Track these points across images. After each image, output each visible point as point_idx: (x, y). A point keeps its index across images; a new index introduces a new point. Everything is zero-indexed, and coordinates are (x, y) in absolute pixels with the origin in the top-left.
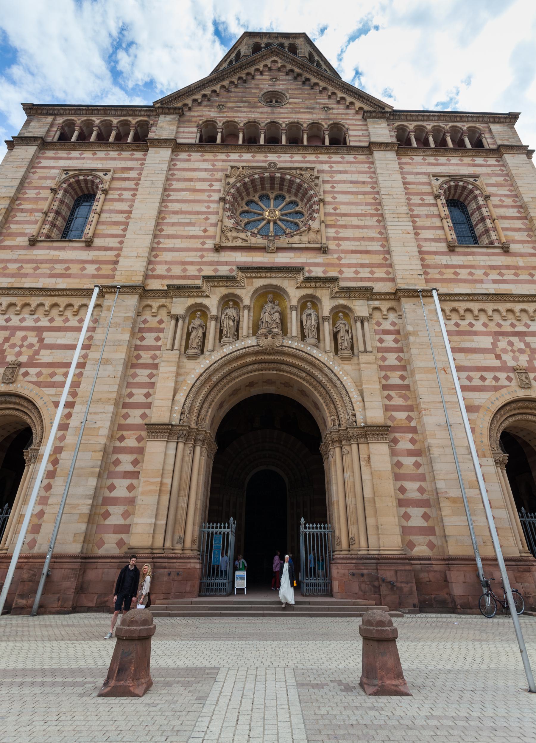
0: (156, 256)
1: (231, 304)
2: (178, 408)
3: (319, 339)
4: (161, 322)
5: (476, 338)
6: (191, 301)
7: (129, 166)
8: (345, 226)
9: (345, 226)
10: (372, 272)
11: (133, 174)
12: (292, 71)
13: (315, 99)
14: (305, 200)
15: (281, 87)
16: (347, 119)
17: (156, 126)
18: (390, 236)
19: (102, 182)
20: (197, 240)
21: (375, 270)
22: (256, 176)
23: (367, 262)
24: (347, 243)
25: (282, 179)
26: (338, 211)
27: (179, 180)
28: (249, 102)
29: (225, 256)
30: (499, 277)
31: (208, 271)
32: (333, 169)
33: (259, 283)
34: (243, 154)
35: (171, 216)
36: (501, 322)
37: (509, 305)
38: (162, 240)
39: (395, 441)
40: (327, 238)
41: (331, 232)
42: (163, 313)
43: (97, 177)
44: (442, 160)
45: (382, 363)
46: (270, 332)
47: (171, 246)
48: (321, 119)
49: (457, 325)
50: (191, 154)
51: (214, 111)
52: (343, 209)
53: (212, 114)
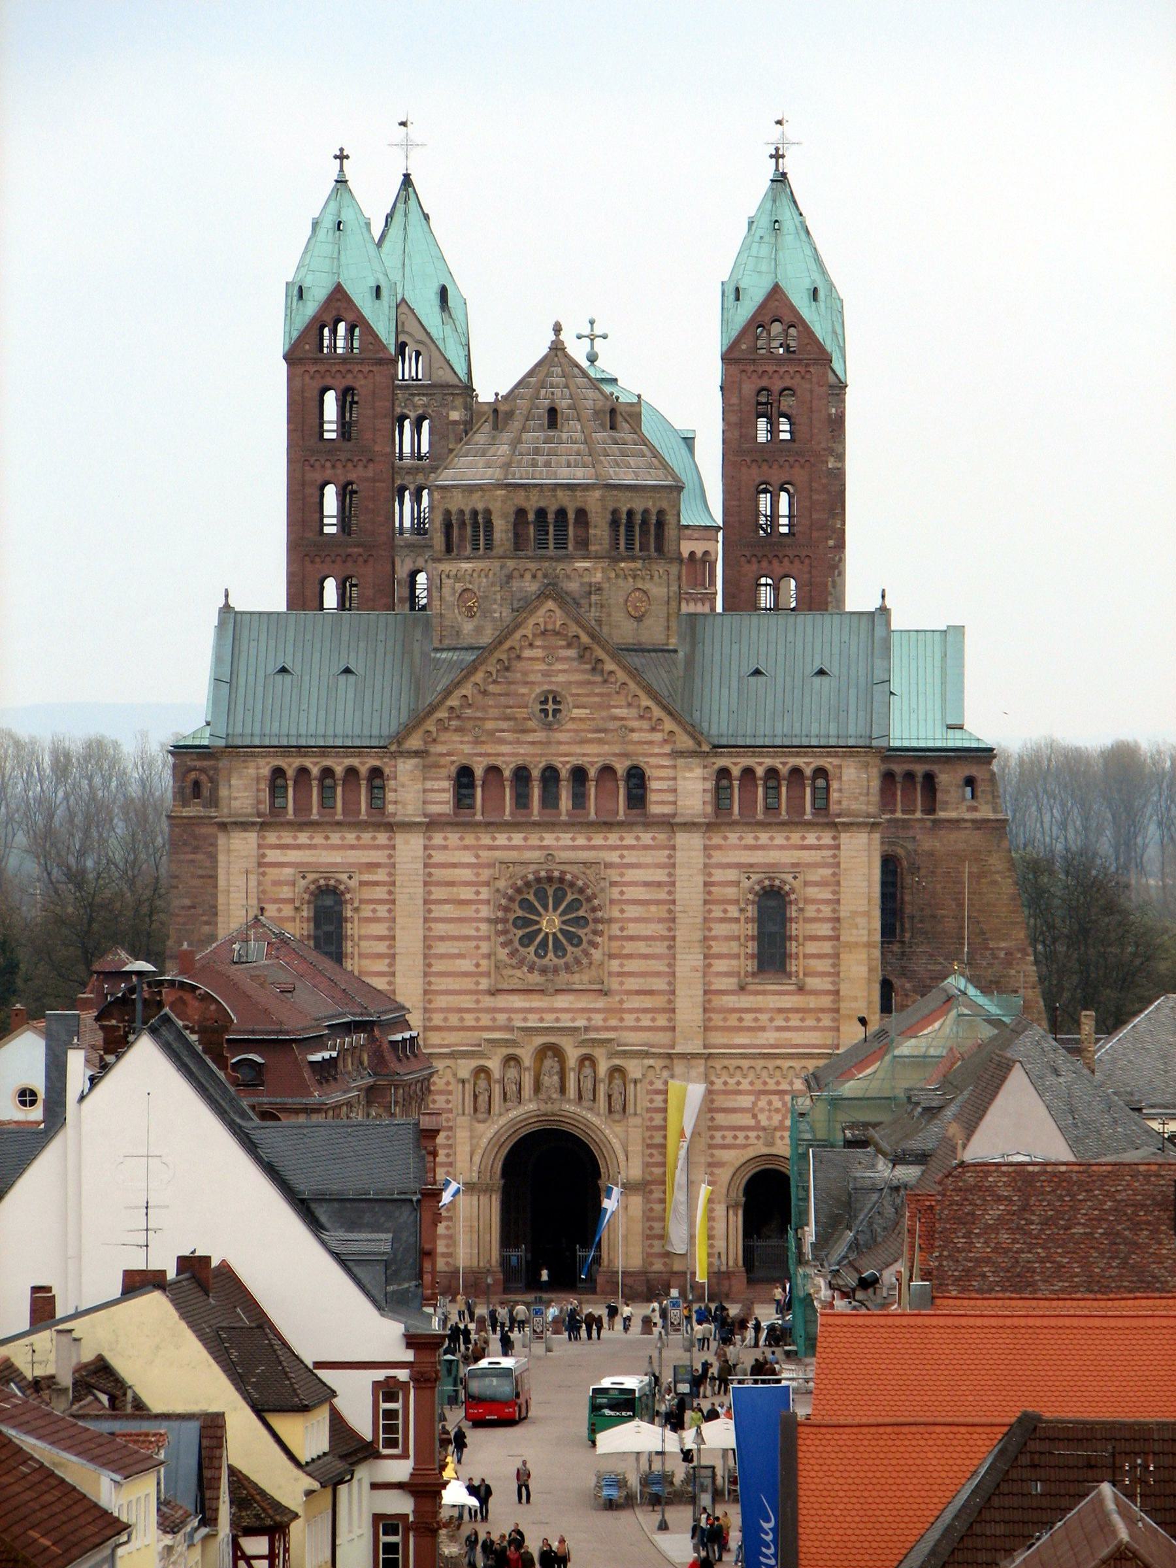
0: (430, 1002)
1: (512, 1063)
2: (475, 1168)
3: (594, 1100)
4: (448, 1083)
5: (739, 1098)
6: (474, 1063)
7: (375, 861)
8: (630, 956)
9: (630, 956)
10: (654, 1020)
11: (381, 875)
12: (577, 637)
13: (610, 707)
14: (589, 906)
15: (561, 678)
16: (651, 755)
17: (395, 778)
18: (677, 974)
19: (348, 890)
20: (469, 979)
21: (656, 1016)
22: (531, 877)
23: (650, 1006)
24: (632, 980)
25: (561, 880)
26: (625, 933)
27: (439, 884)
28: (515, 719)
29: (502, 1001)
30: (784, 1024)
31: (485, 1020)
32: (625, 861)
33: (540, 1040)
34: (513, 835)
35: (438, 943)
36: (768, 1080)
37: (779, 1062)
38: (433, 979)
39: (651, 1192)
40: (610, 974)
41: (615, 965)
42: (449, 1076)
43: (339, 882)
44: (764, 837)
45: (649, 1124)
46: (550, 1098)
47: (443, 987)
48: (615, 755)
49: (725, 1083)
50: (449, 835)
51: (468, 742)
52: (633, 929)
53: (467, 749)
